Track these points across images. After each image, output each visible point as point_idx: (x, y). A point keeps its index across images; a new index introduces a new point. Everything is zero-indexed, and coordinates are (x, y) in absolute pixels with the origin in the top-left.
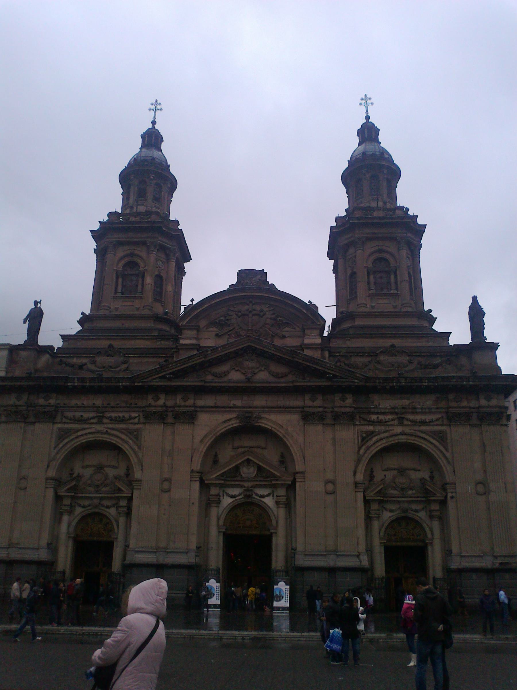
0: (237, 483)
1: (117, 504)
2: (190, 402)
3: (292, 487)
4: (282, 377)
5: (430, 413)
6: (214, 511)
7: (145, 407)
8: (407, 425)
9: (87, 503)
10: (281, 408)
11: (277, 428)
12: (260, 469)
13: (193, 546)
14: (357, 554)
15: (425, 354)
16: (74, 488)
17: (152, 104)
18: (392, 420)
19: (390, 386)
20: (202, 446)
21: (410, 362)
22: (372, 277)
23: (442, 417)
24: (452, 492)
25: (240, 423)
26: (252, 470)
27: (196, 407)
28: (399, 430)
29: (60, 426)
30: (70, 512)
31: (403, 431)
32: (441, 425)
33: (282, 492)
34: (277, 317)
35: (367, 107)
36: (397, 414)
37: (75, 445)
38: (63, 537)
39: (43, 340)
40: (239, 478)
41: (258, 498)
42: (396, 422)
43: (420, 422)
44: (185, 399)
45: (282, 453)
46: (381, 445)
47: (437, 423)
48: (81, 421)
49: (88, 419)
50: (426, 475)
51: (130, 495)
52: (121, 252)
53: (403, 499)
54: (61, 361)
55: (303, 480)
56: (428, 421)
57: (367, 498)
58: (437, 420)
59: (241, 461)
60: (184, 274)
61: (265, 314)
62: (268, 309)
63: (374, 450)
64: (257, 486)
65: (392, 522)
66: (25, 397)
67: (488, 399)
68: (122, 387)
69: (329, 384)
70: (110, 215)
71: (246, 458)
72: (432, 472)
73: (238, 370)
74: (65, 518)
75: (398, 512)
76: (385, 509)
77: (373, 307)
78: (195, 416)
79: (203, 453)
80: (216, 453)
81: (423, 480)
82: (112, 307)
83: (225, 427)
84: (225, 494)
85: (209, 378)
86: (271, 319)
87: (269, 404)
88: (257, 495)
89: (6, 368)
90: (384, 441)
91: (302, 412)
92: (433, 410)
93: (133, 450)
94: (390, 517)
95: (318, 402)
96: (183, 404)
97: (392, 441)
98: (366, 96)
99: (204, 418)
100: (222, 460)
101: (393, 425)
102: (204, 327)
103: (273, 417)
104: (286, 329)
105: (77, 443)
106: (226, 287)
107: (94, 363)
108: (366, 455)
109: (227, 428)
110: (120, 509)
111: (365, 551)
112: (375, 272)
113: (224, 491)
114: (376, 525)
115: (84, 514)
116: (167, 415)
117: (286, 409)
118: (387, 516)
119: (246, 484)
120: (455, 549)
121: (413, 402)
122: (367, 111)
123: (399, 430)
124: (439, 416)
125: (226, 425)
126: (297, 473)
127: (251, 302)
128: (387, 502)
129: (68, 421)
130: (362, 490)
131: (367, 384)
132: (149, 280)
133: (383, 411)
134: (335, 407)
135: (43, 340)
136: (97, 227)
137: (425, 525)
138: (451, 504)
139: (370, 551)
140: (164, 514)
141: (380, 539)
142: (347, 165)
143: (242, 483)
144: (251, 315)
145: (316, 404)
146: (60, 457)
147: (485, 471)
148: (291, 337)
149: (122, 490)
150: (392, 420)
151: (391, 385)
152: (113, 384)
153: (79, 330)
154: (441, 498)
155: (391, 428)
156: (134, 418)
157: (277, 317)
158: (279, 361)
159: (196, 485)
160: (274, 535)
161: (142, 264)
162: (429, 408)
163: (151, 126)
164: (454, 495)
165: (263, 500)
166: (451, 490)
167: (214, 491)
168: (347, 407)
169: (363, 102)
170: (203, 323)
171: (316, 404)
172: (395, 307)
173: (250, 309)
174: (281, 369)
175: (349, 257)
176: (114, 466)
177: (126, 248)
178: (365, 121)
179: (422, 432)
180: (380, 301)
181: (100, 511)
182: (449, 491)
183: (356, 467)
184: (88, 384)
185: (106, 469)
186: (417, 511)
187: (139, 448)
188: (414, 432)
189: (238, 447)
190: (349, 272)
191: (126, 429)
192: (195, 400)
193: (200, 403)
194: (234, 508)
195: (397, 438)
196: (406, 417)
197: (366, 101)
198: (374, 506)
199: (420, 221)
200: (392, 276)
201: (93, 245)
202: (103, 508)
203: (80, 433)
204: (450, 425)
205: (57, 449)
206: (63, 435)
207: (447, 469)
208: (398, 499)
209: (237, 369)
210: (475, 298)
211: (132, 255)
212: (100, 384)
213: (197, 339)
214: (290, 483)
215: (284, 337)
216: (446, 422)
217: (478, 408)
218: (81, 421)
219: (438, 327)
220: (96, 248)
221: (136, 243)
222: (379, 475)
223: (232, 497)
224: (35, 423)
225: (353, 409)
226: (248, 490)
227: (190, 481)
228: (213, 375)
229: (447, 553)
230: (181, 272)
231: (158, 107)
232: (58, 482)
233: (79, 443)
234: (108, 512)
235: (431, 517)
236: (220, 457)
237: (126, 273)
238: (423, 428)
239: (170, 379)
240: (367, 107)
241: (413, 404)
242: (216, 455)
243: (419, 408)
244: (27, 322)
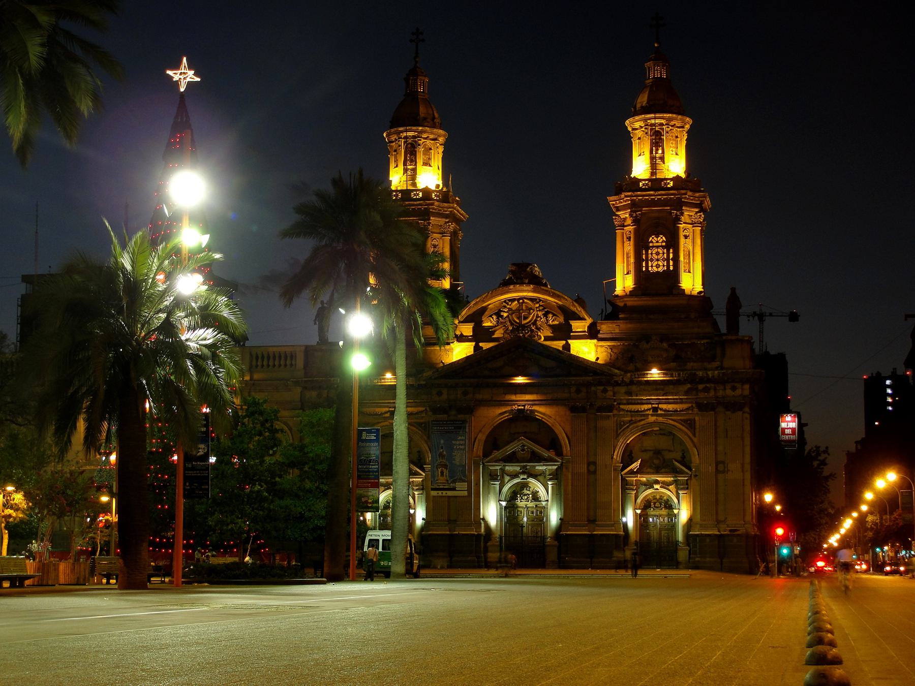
5: (682, 403)
17: (413, 34)
23: (692, 406)
42: (651, 412)
49: (382, 414)
56: (679, 410)
67: (734, 389)
124: (690, 405)
193: (479, 396)
210: (733, 290)
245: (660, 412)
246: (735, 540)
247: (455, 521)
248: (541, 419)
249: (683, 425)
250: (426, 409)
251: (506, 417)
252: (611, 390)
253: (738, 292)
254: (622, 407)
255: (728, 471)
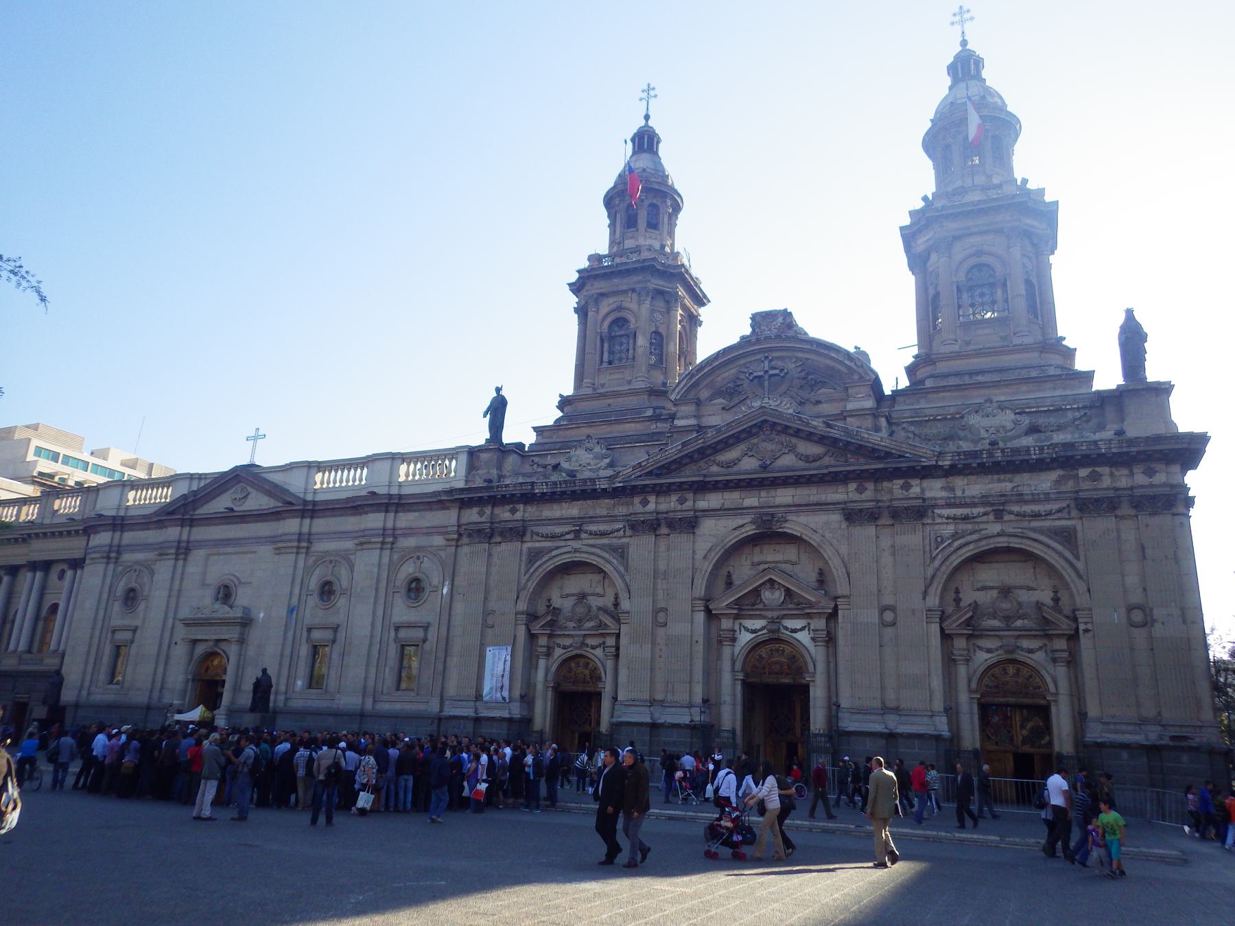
0: (758, 613)
1: (604, 643)
2: (689, 504)
3: (833, 616)
4: (814, 461)
6: (727, 651)
7: (630, 515)
8: (1011, 521)
9: (567, 642)
10: (815, 505)
11: (810, 535)
12: (788, 590)
13: (698, 699)
14: (930, 713)
15: (1046, 409)
16: (552, 624)
18: (985, 514)
19: (979, 464)
20: (707, 563)
21: (1016, 423)
22: (965, 296)
23: (1068, 506)
24: (1086, 623)
25: (755, 529)
26: (777, 594)
27: (696, 511)
28: (996, 528)
29: (530, 545)
30: (548, 654)
31: (1002, 530)
32: (1067, 519)
33: (820, 623)
34: (808, 374)
35: (962, 26)
36: (992, 505)
37: (548, 569)
38: (540, 687)
39: (508, 437)
40: (761, 606)
41: (788, 633)
42: (991, 517)
43: (1029, 516)
44: (682, 501)
45: (820, 569)
46: (965, 553)
47: (1060, 515)
48: (553, 537)
49: (562, 535)
50: (1046, 597)
51: (618, 632)
52: (606, 306)
53: (1006, 633)
54: (533, 460)
55: (847, 607)
57: (947, 632)
58: (1059, 511)
59: (761, 581)
60: (700, 324)
61: (787, 373)
62: (794, 365)
63: (955, 560)
64: (785, 617)
65: (990, 667)
66: (488, 510)
67: (1150, 473)
68: (599, 490)
69: (881, 466)
70: (590, 258)
71: (767, 578)
72: (1056, 592)
73: (752, 456)
74: (542, 663)
75: (999, 652)
76: (980, 648)
77: (968, 343)
78: (696, 523)
79: (707, 574)
80: (729, 572)
81: (1039, 606)
82: (596, 383)
83: (737, 536)
84: (742, 629)
85: (714, 469)
86: (799, 378)
87: (797, 501)
88: (786, 628)
89: (466, 477)
90: (972, 546)
91: (843, 509)
92: (1052, 496)
93: (618, 572)
94: (986, 660)
95: (868, 494)
96: (679, 507)
97: (985, 545)
98: (961, 7)
99: (708, 527)
100: (737, 582)
101: (987, 522)
102: (707, 399)
103: (803, 519)
104: (823, 390)
105: (550, 565)
106: (735, 340)
107: (569, 460)
108: (944, 568)
109: (740, 537)
110: (607, 650)
111: (942, 709)
112: (971, 289)
113: (740, 624)
114: (962, 670)
115: (564, 657)
116: (659, 525)
117: (820, 507)
118: (982, 659)
119: (769, 614)
120: (1093, 710)
121: (1018, 486)
122: (963, 33)
123: (996, 528)
124: (1064, 504)
125: (737, 533)
126: (839, 597)
127: (767, 357)
128: (981, 637)
129: (540, 539)
130: (938, 620)
131: (940, 463)
132: (642, 341)
133: (968, 501)
134: (894, 500)
135: (508, 437)
136: (574, 277)
137: (1043, 672)
138: (1085, 641)
139: (951, 711)
140: (660, 657)
141: (970, 691)
142: (929, 125)
143: (763, 613)
144: (766, 377)
145: (864, 496)
146: (532, 585)
147: (1145, 590)
148: (826, 402)
149: (608, 626)
150: (985, 514)
151: (979, 461)
152: (589, 487)
153: (557, 417)
154: (1068, 632)
155: (982, 526)
156: (618, 530)
157: (808, 374)
158: (809, 437)
159: (700, 617)
160: (811, 684)
161: (632, 320)
162: (1045, 494)
163: (643, 123)
164: (1089, 627)
165: (794, 635)
166: (1086, 620)
167: (726, 624)
168: (912, 498)
169: (958, 18)
170: (704, 394)
171: (864, 496)
172: (1003, 338)
173: (766, 369)
174: (814, 449)
175: (930, 269)
176: (598, 594)
177: (611, 300)
178: (960, 49)
179: (1034, 530)
180: (980, 332)
181: (585, 653)
182: (1080, 620)
183: (927, 587)
184: (559, 490)
185: (589, 598)
186: (1031, 651)
187: (627, 570)
188: (1020, 530)
189: (759, 564)
190: (931, 292)
191: (610, 546)
192: (694, 501)
193: (702, 504)
194: (755, 647)
195: (991, 541)
196: (1006, 508)
197: (962, 16)
198: (960, 643)
199: (1048, 198)
200: (999, 292)
201: (573, 300)
202: (588, 649)
203: (554, 553)
204: (1081, 518)
205: (527, 576)
206: (534, 556)
207: (1078, 586)
208: (997, 633)
209: (750, 454)
210: (1130, 314)
211: (620, 308)
212: (573, 489)
213: (697, 417)
214: (830, 611)
215: (818, 402)
216: (1074, 513)
217: (1132, 488)
218: (553, 537)
219: (1080, 365)
220: (576, 306)
221: (625, 292)
222: (968, 597)
223: (753, 631)
224: (500, 543)
225: (921, 501)
226: (772, 621)
227: (692, 611)
228: (719, 464)
229: (1080, 717)
230: (693, 321)
231: (652, 93)
232: (532, 617)
233: (553, 566)
234: (593, 655)
235: (1054, 660)
236: (734, 577)
237: (613, 334)
238: (1035, 524)
239: (659, 476)
240: (962, 26)
241: (1019, 488)
242: (729, 575)
243: (1027, 494)
244: (488, 416)
245: (1006, 518)
246: (1185, 758)
247: (662, 701)
248: (799, 535)
249: (1055, 541)
250: (624, 527)
251: (744, 533)
252: (917, 485)
253: (1138, 316)
254: (935, 511)
255: (1154, 621)
